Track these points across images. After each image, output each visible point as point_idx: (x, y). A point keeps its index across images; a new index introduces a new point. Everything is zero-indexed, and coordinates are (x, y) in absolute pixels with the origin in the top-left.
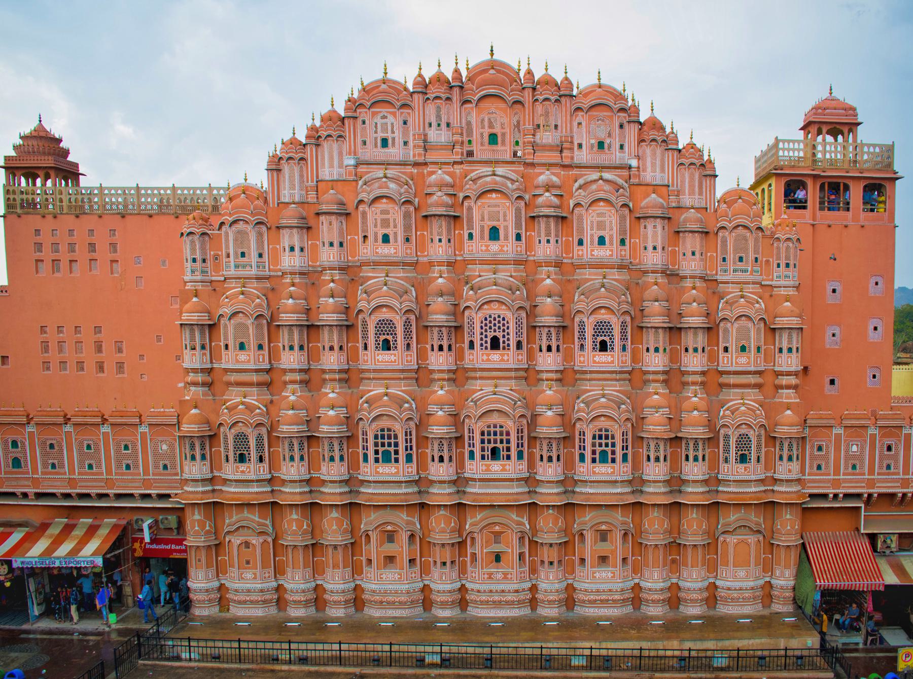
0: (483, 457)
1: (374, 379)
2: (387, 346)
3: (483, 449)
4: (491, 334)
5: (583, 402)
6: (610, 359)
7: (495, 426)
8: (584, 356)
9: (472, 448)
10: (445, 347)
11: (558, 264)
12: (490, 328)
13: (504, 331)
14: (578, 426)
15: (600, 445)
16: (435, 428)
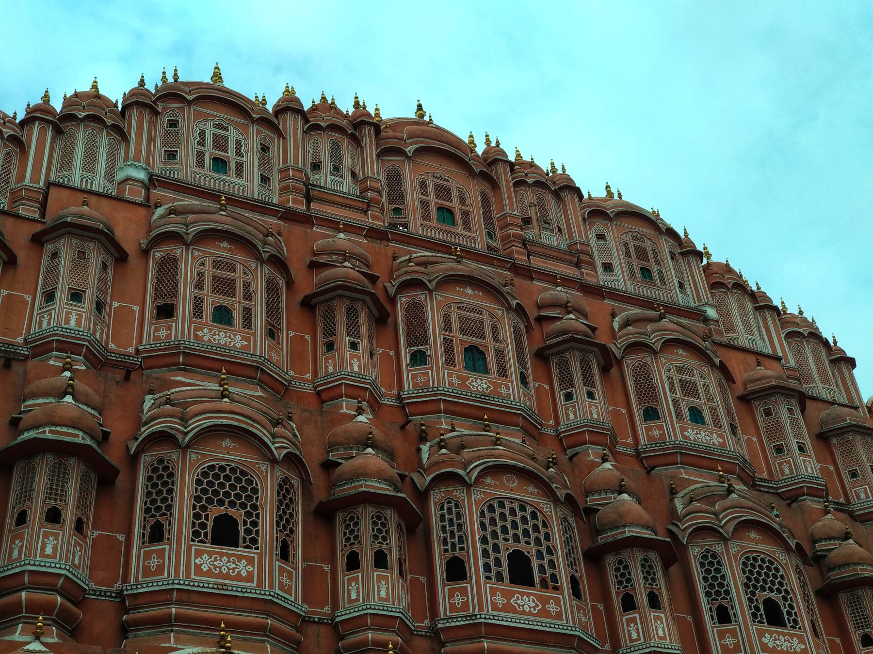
1: (179, 618)
4: (507, 547)
8: (733, 633)
12: (504, 530)
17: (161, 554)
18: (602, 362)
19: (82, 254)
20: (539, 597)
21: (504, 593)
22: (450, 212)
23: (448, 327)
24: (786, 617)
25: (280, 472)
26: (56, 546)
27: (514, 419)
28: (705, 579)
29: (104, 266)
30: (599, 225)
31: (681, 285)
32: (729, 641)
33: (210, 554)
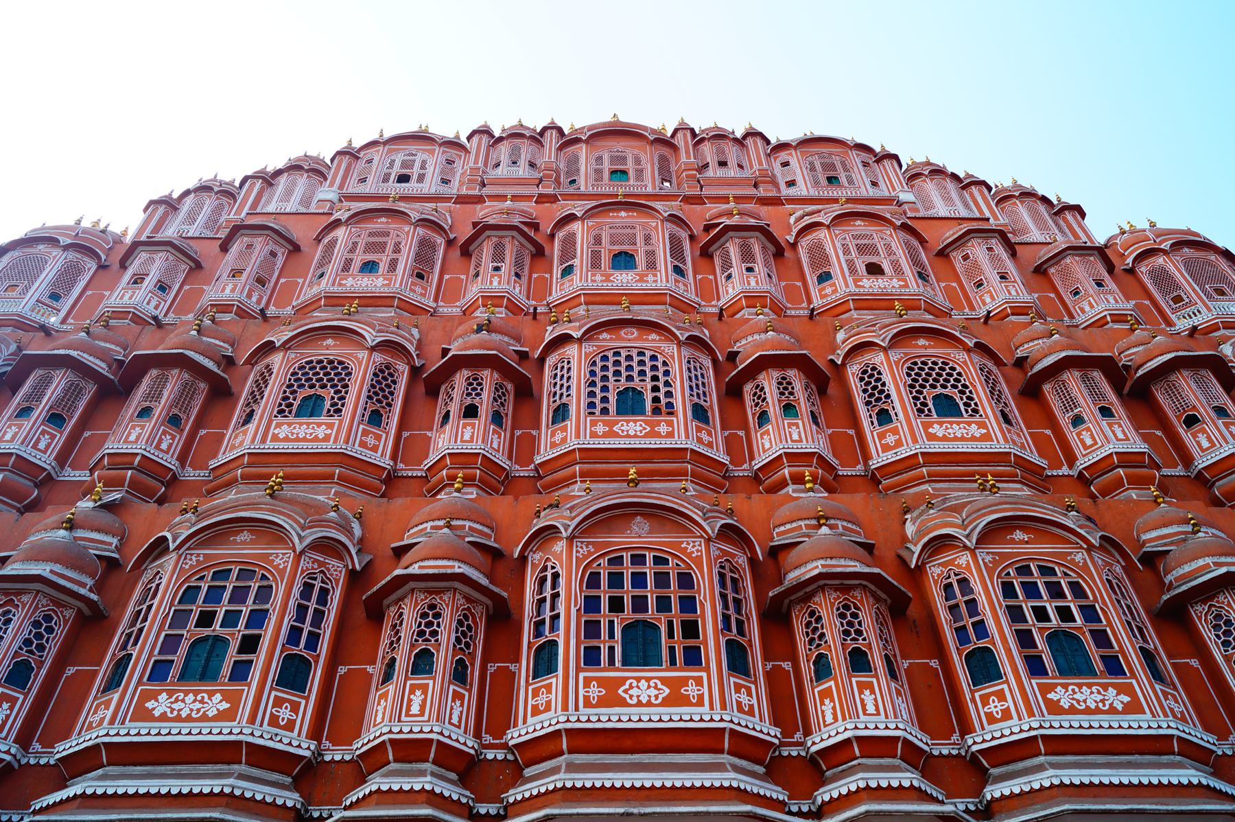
0: (591, 657)
2: (311, 407)
3: (592, 629)
5: (930, 505)
6: (975, 430)
7: (638, 560)
8: (895, 431)
9: (548, 635)
10: (484, 410)
11: (777, 309)
12: (617, 373)
13: (655, 378)
14: (935, 570)
15: (1041, 614)
16: (416, 566)
17: (245, 433)
18: (772, 248)
19: (249, 246)
20: (646, 422)
21: (605, 423)
22: (624, 172)
23: (598, 240)
24: (962, 408)
25: (378, 358)
26: (140, 434)
27: (662, 299)
28: (865, 391)
29: (273, 254)
30: (783, 156)
31: (874, 184)
32: (890, 439)
33: (289, 425)
